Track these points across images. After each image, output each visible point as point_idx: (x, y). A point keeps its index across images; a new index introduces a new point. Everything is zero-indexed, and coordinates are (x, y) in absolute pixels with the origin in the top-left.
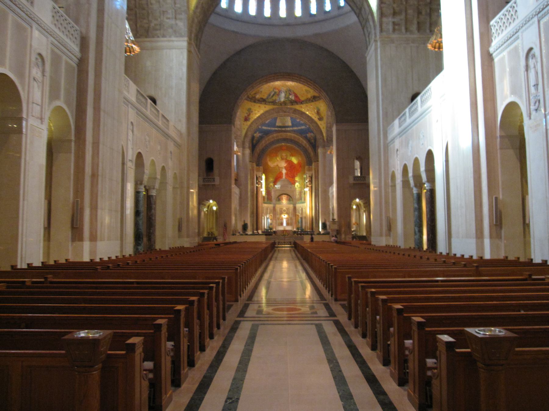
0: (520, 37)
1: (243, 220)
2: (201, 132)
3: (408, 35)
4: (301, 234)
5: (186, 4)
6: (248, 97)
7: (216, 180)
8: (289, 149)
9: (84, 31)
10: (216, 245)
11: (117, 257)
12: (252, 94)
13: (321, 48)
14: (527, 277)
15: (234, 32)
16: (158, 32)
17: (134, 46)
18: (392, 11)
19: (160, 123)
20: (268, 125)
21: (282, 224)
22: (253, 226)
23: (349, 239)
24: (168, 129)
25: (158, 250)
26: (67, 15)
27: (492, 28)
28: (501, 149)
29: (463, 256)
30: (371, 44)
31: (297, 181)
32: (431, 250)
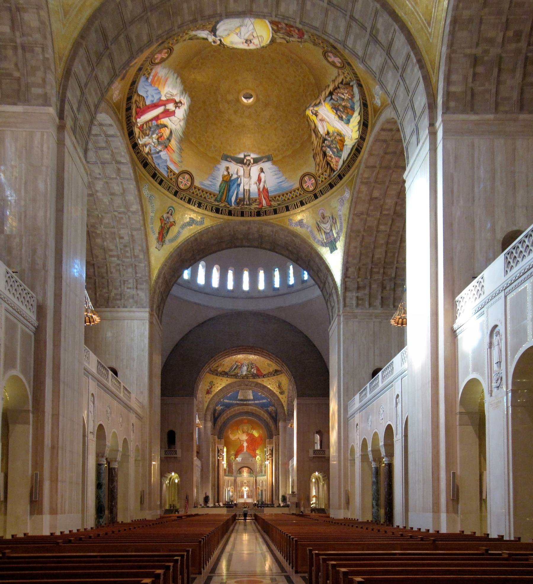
0: (485, 312)
1: (204, 493)
2: (163, 404)
3: (371, 310)
4: (261, 507)
5: (147, 274)
6: (210, 370)
7: (178, 452)
8: (250, 422)
9: (40, 299)
10: (178, 517)
11: (78, 530)
12: (214, 366)
13: (284, 322)
14: (484, 552)
15: (195, 303)
16: (118, 302)
17: (94, 316)
18: (356, 286)
19: (121, 395)
20: (229, 399)
21: (242, 497)
22: (214, 497)
23: (307, 512)
24: (130, 401)
25: (120, 522)
26: (21, 280)
27: (458, 303)
28: (460, 425)
29: (420, 529)
30: (334, 318)
31: (257, 454)
32: (388, 523)
